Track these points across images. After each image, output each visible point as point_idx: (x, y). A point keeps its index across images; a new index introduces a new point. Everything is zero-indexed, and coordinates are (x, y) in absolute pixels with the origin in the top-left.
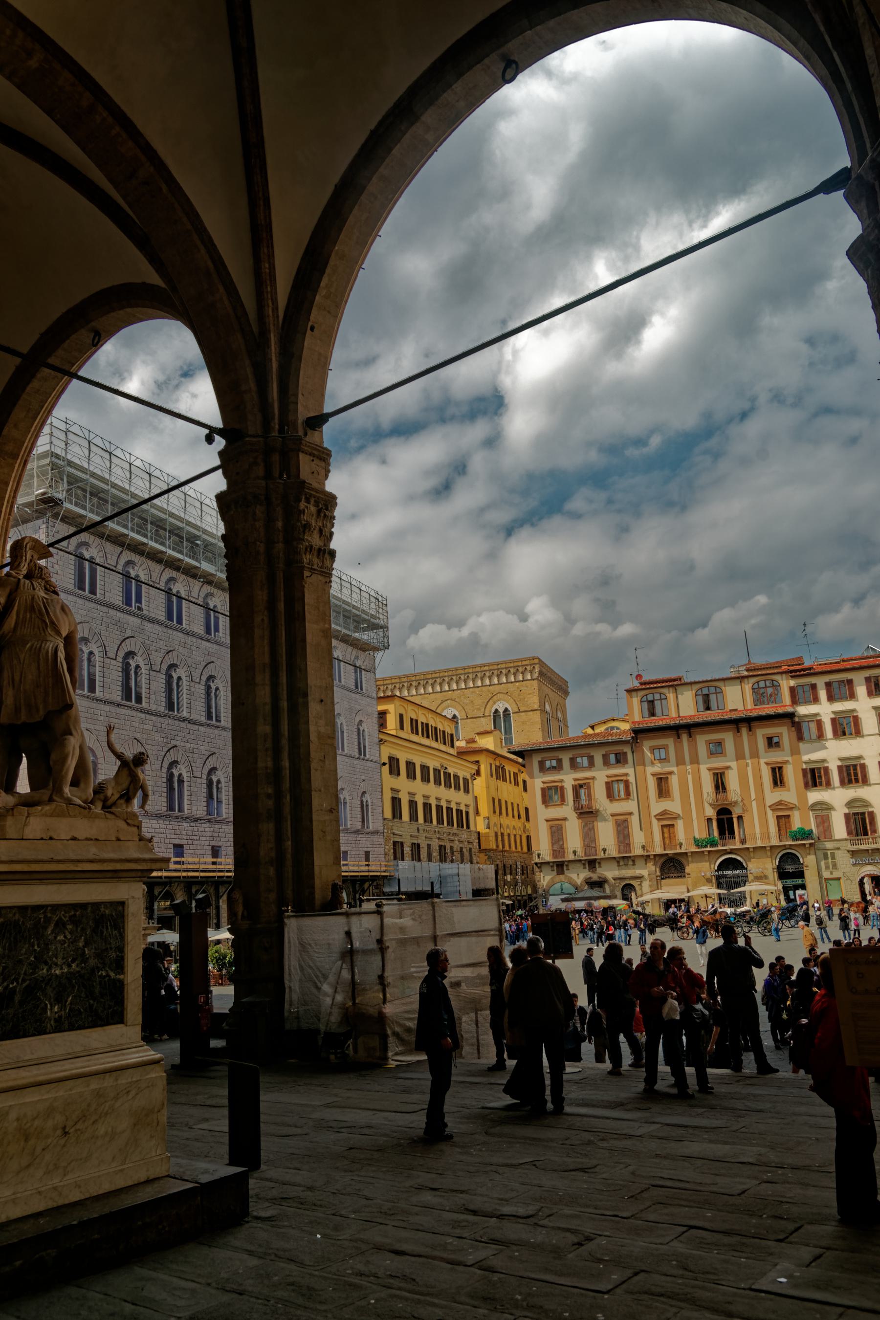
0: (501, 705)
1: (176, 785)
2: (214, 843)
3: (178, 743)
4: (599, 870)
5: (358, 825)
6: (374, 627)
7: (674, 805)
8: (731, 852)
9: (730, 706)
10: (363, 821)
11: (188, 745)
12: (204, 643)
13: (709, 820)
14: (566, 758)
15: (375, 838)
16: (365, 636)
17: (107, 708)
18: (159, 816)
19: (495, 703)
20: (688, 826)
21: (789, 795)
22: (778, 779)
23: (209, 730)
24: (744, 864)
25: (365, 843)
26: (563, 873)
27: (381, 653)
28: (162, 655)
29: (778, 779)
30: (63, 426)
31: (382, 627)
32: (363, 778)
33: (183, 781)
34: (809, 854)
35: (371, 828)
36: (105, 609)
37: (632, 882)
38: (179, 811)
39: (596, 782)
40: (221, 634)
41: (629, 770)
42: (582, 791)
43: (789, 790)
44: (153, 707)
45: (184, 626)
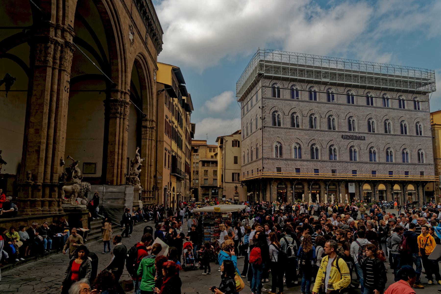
1: (315, 151)
2: (333, 169)
3: (315, 138)
5: (416, 162)
6: (426, 84)
10: (419, 160)
11: (320, 138)
12: (327, 105)
15: (428, 167)
16: (422, 89)
17: (285, 130)
18: (307, 161)
23: (329, 133)
25: (420, 169)
27: (431, 93)
28: (308, 111)
30: (263, 52)
31: (430, 83)
32: (419, 144)
33: (318, 150)
35: (425, 162)
36: (284, 101)
38: (316, 159)
40: (335, 101)
44: (304, 128)
45: (317, 100)
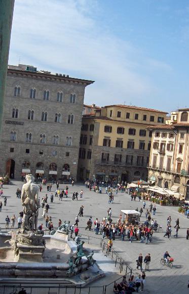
7: (181, 156)
42: (163, 146)
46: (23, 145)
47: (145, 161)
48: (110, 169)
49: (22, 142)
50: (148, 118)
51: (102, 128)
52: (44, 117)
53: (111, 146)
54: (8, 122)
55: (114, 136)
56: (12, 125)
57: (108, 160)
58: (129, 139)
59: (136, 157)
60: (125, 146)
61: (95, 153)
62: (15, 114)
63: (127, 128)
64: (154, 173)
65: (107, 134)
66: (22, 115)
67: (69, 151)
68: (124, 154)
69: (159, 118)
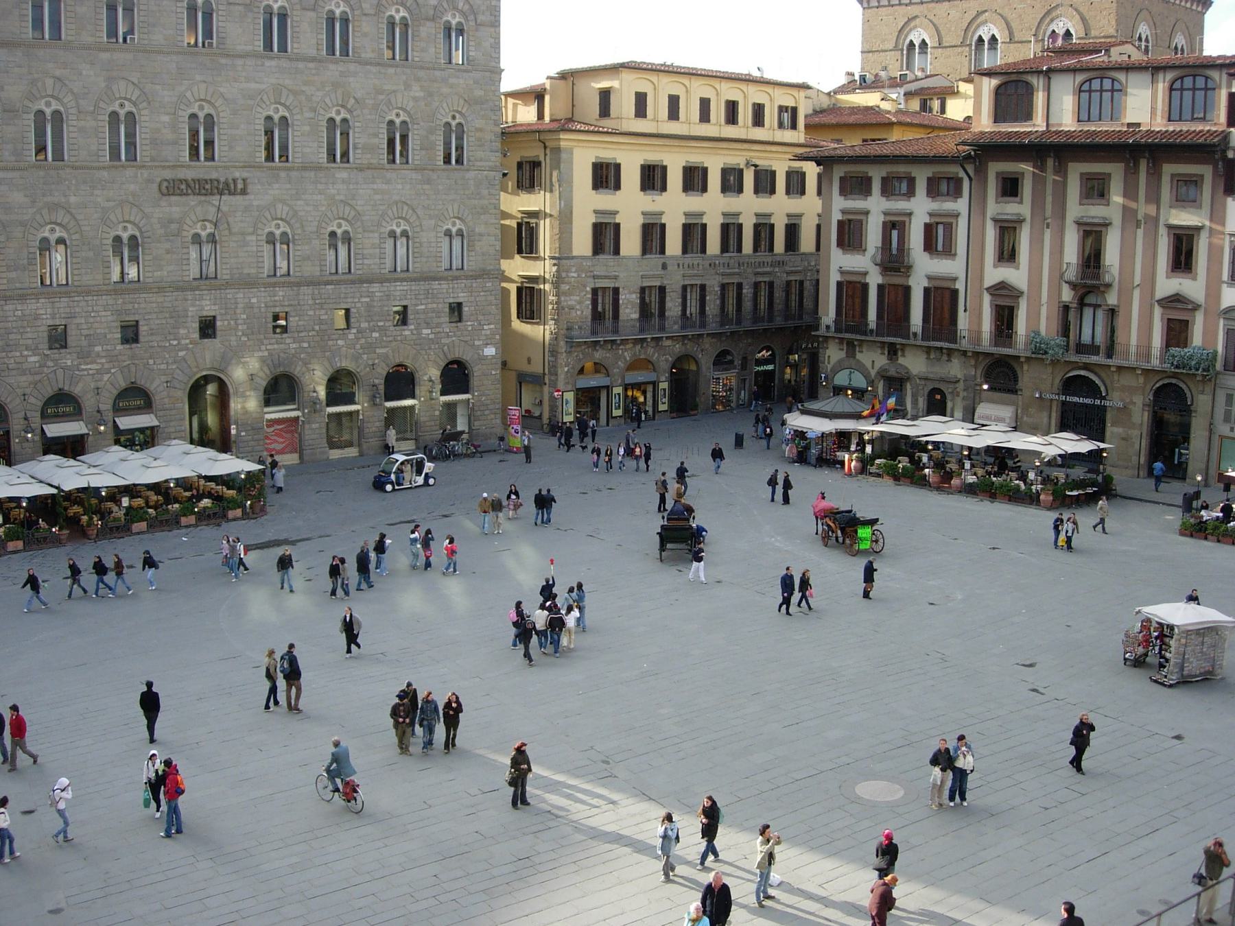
0: (1061, 24)
4: (901, 360)
7: (1017, 276)
8: (1086, 367)
9: (1130, 118)
13: (1066, 308)
14: (877, 174)
19: (1052, 20)
20: (1033, 316)
21: (1192, 287)
22: (1182, 260)
24: (1103, 389)
26: (854, 356)
29: (1182, 260)
34: (1202, 392)
37: (943, 387)
39: (913, 218)
41: (961, 205)
42: (895, 233)
43: (1195, 279)
46: (258, 298)
47: (808, 303)
48: (628, 355)
49: (249, 283)
50: (718, 111)
51: (582, 175)
52: (397, 143)
53: (622, 253)
54: (173, 188)
55: (630, 206)
56: (193, 200)
57: (616, 315)
58: (686, 214)
59: (717, 289)
60: (631, 243)
61: (565, 294)
62: (202, 139)
63: (631, 164)
64: (851, 354)
65: (605, 200)
66: (239, 143)
67: (462, 297)
68: (674, 282)
69: (782, 109)
